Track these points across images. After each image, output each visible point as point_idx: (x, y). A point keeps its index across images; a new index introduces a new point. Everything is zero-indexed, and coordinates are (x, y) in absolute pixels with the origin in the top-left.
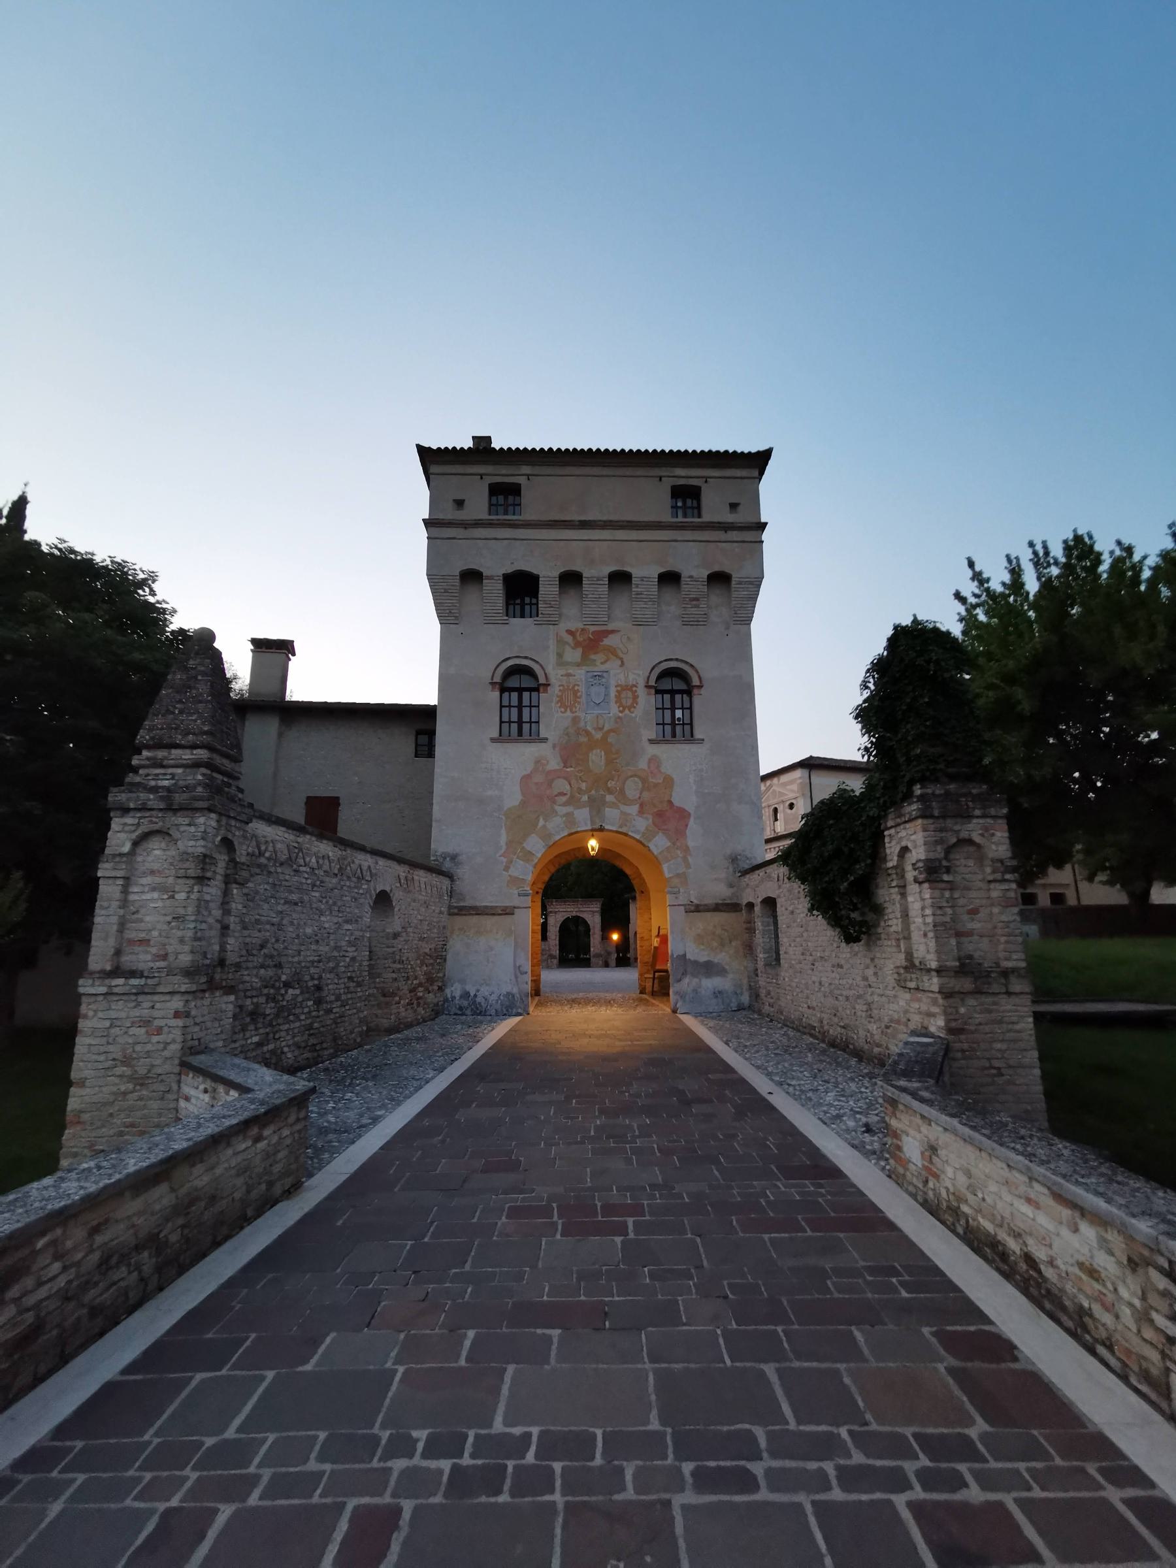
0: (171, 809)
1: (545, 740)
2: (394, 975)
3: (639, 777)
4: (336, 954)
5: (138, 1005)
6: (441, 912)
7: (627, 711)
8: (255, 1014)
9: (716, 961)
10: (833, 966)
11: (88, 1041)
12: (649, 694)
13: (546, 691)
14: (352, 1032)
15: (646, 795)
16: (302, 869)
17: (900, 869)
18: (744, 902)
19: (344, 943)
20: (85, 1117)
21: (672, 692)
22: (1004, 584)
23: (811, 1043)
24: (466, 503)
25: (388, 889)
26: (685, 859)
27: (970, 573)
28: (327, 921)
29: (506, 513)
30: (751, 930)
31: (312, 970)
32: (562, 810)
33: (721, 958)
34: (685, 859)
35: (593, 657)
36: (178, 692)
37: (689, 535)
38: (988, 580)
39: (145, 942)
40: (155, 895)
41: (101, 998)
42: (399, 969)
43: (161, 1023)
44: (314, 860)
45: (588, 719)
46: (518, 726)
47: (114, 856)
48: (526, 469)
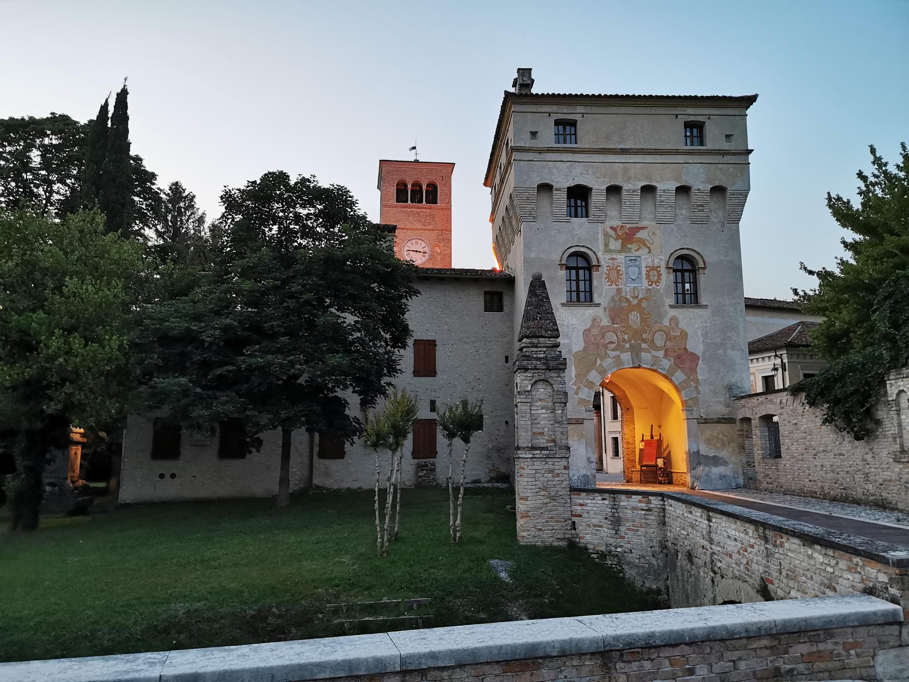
0: (549, 369)
1: (598, 305)
5: (547, 463)
7: (654, 285)
11: (527, 479)
13: (598, 270)
15: (668, 343)
17: (897, 402)
20: (530, 514)
21: (683, 271)
22: (898, 166)
26: (696, 388)
27: (872, 158)
29: (565, 143)
30: (749, 436)
33: (724, 454)
35: (629, 246)
37: (697, 159)
38: (886, 164)
39: (542, 434)
40: (544, 411)
43: (559, 472)
45: (627, 289)
46: (582, 295)
48: (580, 109)
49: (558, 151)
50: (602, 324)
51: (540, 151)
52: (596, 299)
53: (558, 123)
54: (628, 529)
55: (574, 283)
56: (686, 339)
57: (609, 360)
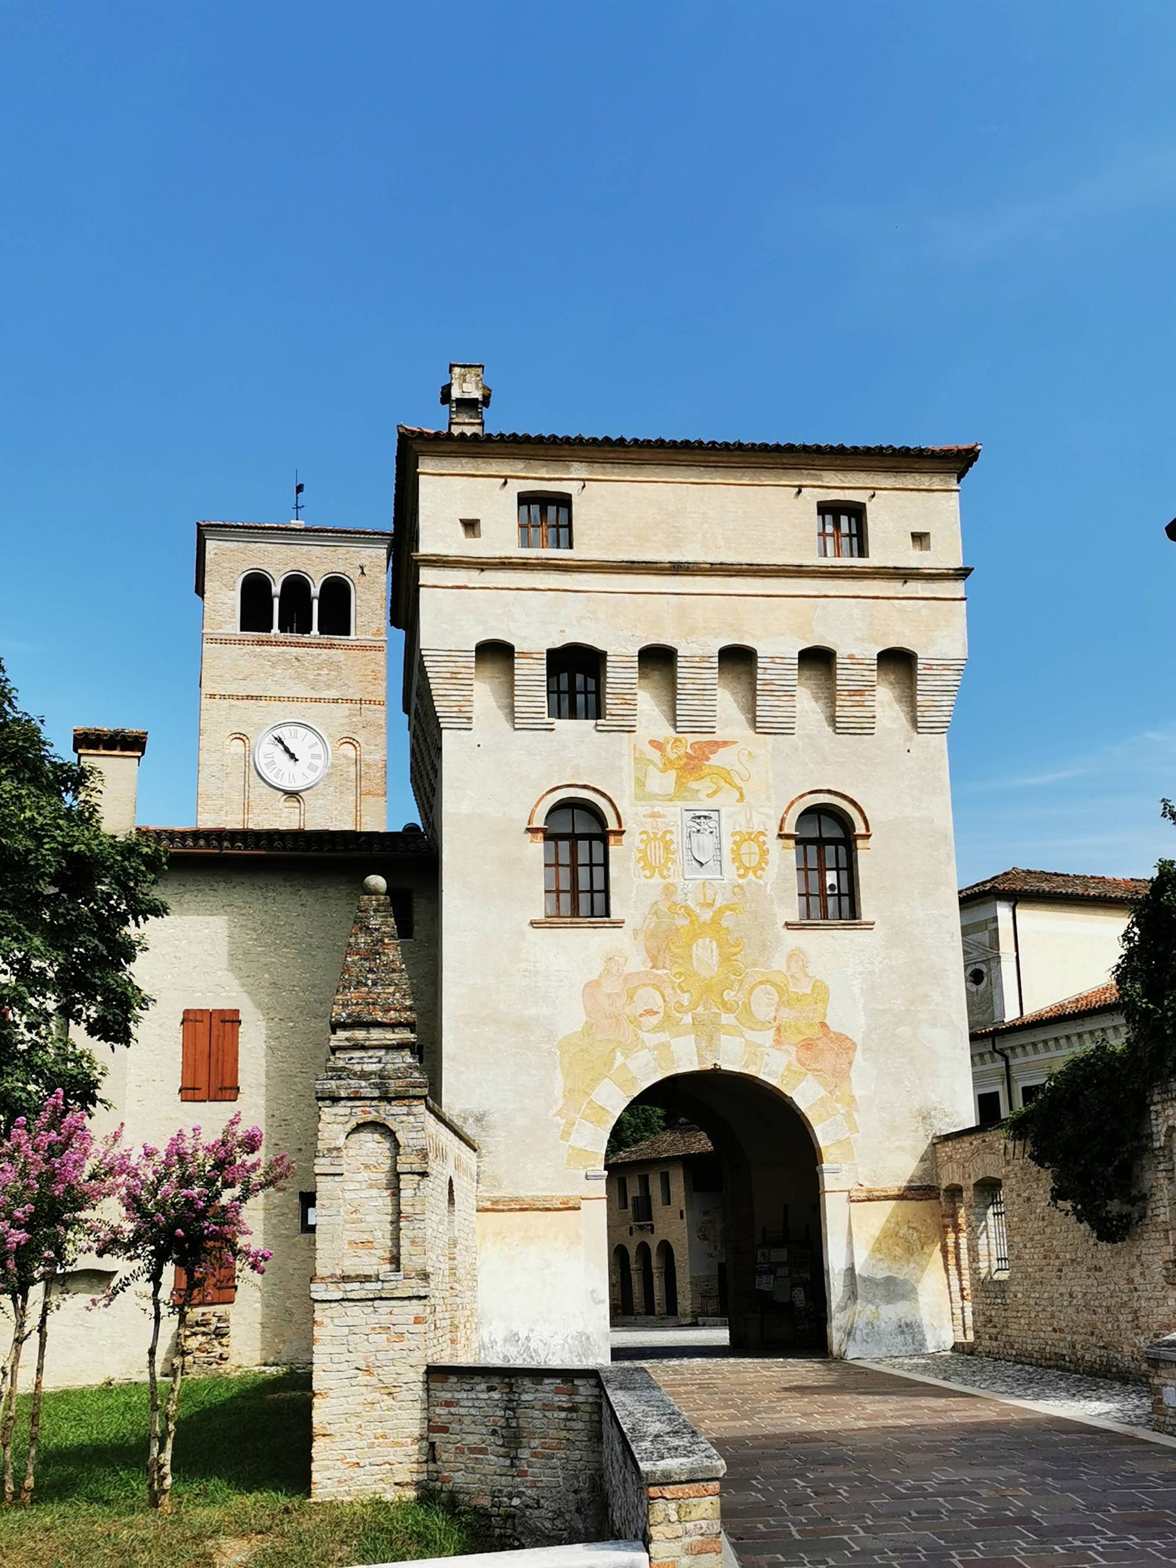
0: (386, 1098)
3: (774, 984)
7: (751, 875)
9: (902, 1278)
10: (1089, 1270)
12: (784, 848)
13: (619, 842)
15: (785, 1014)
18: (944, 1184)
21: (821, 842)
26: (848, 1116)
32: (653, 1039)
34: (848, 1116)
35: (694, 785)
36: (366, 960)
40: (374, 1192)
41: (333, 1305)
45: (688, 883)
47: (329, 1150)
48: (579, 470)
49: (525, 565)
50: (630, 968)
51: (482, 565)
52: (616, 913)
53: (524, 499)
54: (534, 1455)
55: (565, 873)
56: (825, 1001)
57: (644, 1055)
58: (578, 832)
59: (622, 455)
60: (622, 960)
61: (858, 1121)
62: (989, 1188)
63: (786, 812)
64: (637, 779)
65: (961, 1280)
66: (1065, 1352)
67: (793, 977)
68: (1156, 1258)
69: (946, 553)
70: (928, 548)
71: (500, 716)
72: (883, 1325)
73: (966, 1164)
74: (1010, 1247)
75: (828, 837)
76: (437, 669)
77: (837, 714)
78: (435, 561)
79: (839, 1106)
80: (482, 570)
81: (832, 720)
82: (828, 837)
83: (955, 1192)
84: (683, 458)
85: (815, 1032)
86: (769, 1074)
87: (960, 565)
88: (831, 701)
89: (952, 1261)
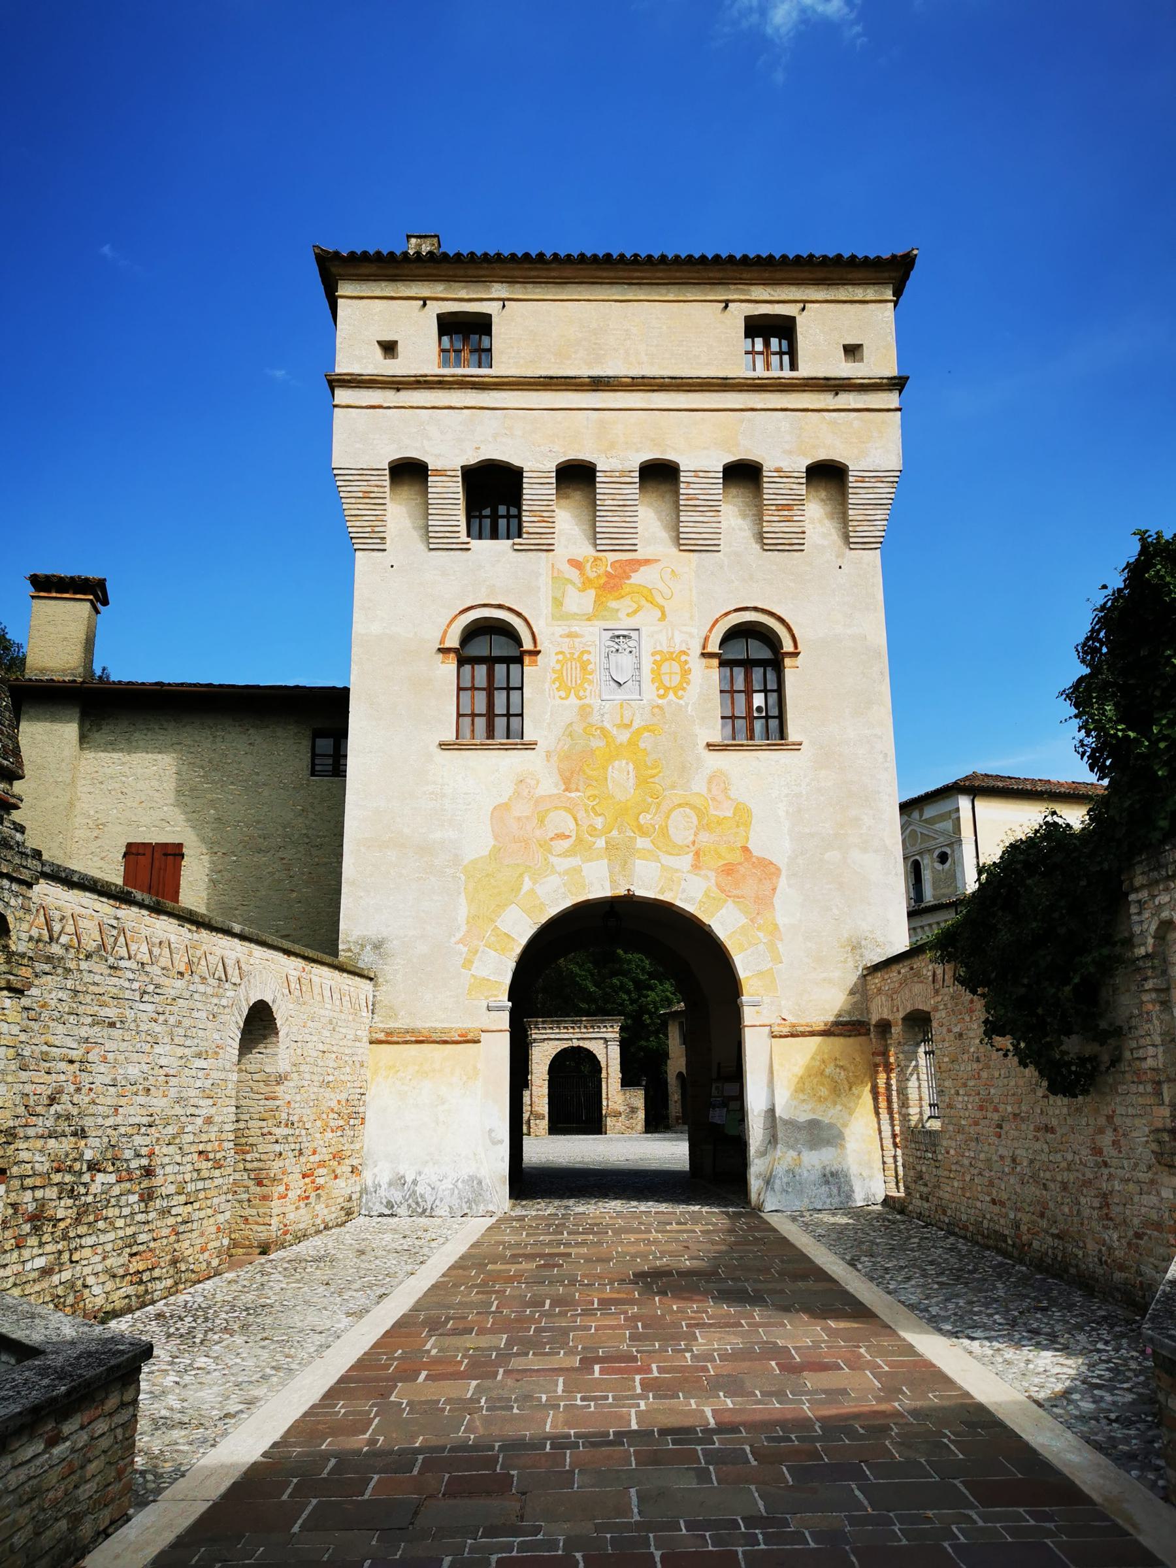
2: (277, 1148)
3: (693, 807)
4: (178, 1110)
6: (357, 1039)
7: (671, 696)
8: (38, 1219)
10: (1037, 1129)
13: (535, 663)
14: (203, 1251)
15: (704, 838)
16: (123, 964)
18: (874, 1018)
19: (192, 1093)
21: (748, 664)
23: (1001, 1264)
24: (400, 348)
25: (268, 999)
28: (167, 1055)
31: (138, 1140)
35: (613, 604)
42: (286, 1137)
44: (144, 948)
45: (606, 705)
51: (397, 384)
56: (748, 824)
57: (554, 880)
58: (491, 650)
59: (544, 273)
60: (533, 782)
61: (781, 950)
62: (919, 1023)
63: (711, 630)
64: (555, 599)
65: (893, 1126)
66: (1006, 1232)
67: (714, 799)
68: (1137, 1122)
69: (881, 361)
70: (861, 360)
71: (415, 537)
72: (806, 1174)
73: (895, 996)
74: (941, 1093)
75: (754, 653)
76: (349, 489)
77: (765, 529)
78: (349, 381)
79: (761, 935)
80: (398, 390)
81: (760, 537)
82: (754, 653)
83: (884, 1027)
84: (605, 274)
85: (737, 857)
86: (686, 900)
87: (894, 372)
88: (759, 519)
89: (883, 1104)
